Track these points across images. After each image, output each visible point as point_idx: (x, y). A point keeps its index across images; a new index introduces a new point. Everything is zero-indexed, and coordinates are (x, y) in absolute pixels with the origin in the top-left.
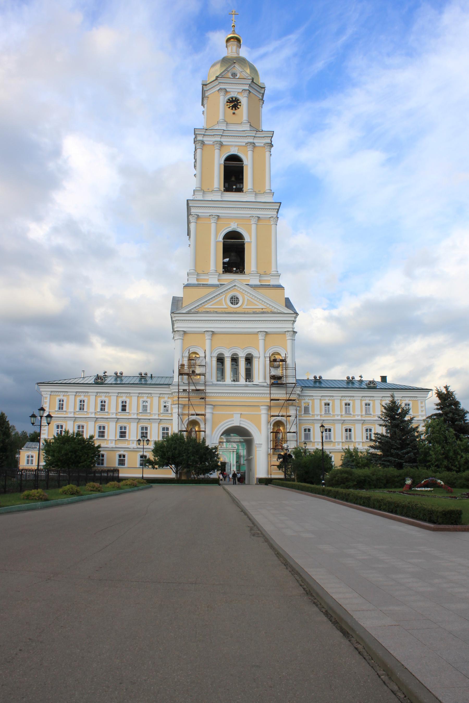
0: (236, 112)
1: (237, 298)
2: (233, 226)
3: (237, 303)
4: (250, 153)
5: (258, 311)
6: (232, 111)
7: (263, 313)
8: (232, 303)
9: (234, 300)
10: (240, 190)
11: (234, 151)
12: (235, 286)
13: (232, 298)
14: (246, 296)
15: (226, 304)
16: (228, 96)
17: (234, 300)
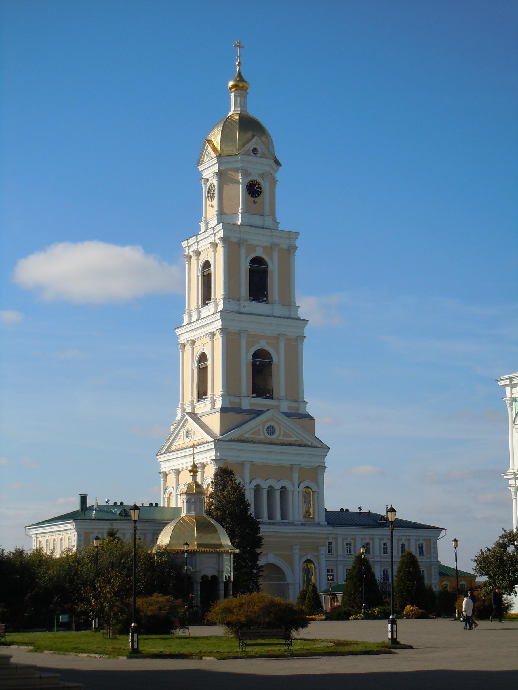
0: (258, 199)
1: (273, 428)
2: (262, 345)
3: (273, 434)
4: (276, 256)
5: (292, 443)
6: (253, 199)
7: (299, 445)
8: (268, 433)
9: (271, 430)
10: (266, 301)
11: (259, 253)
12: (272, 415)
13: (268, 428)
14: (281, 427)
15: (264, 435)
16: (249, 179)
17: (271, 430)
